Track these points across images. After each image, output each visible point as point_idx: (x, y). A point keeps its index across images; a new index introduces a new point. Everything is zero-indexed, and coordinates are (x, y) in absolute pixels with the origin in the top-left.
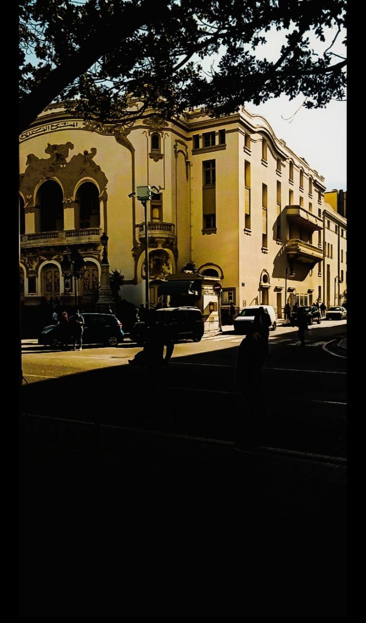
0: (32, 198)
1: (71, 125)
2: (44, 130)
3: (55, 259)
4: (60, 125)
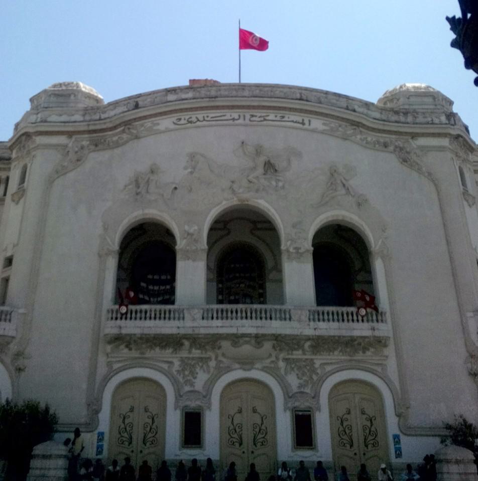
0: (200, 230)
1: (299, 123)
2: (234, 119)
3: (265, 369)
4: (272, 117)
